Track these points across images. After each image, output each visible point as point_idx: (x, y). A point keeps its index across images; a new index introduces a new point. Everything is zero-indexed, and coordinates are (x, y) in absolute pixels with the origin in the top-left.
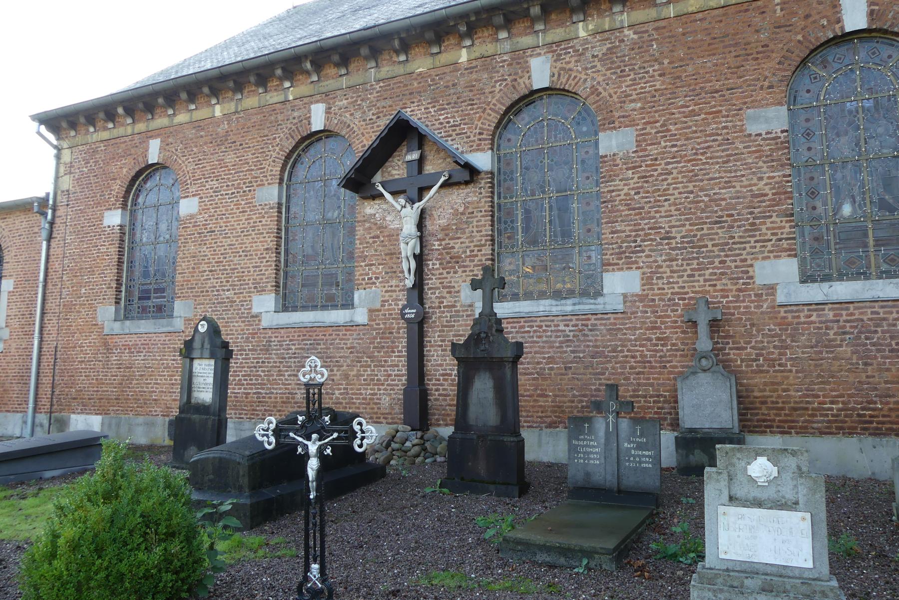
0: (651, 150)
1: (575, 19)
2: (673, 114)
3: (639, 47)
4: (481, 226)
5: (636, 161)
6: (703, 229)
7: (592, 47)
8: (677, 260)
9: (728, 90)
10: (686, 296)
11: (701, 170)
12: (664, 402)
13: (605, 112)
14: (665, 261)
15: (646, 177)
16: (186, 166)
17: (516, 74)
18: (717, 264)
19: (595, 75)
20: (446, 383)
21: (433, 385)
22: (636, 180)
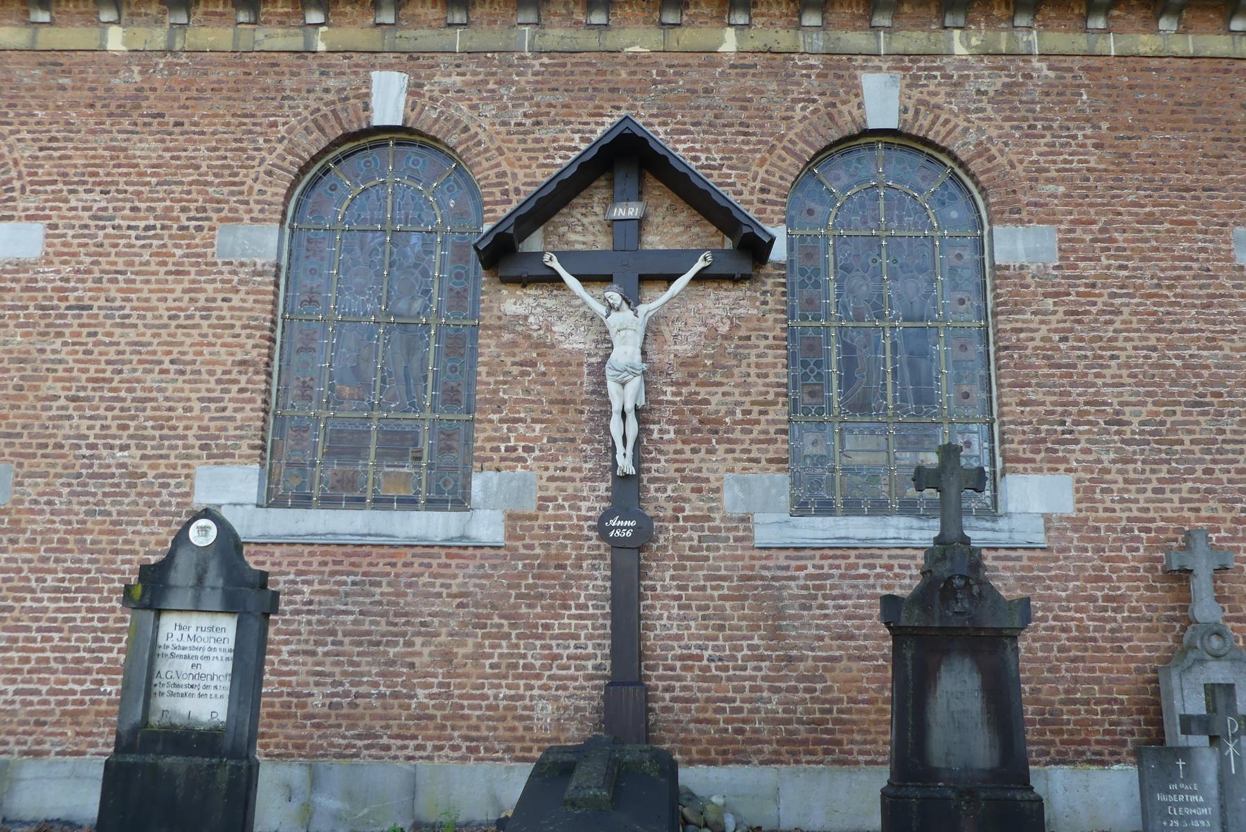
0: (1084, 269)
1: (949, 21)
2: (1120, 214)
3: (1060, 92)
4: (767, 365)
5: (1059, 284)
6: (1174, 413)
7: (977, 77)
8: (1135, 462)
9: (1204, 190)
10: (1153, 526)
11: (1168, 313)
12: (1121, 712)
13: (1003, 190)
14: (1114, 462)
15: (1077, 313)
17: (835, 94)
18: (1199, 474)
19: (984, 125)
20: (689, 675)
21: (660, 678)
22: (1060, 316)
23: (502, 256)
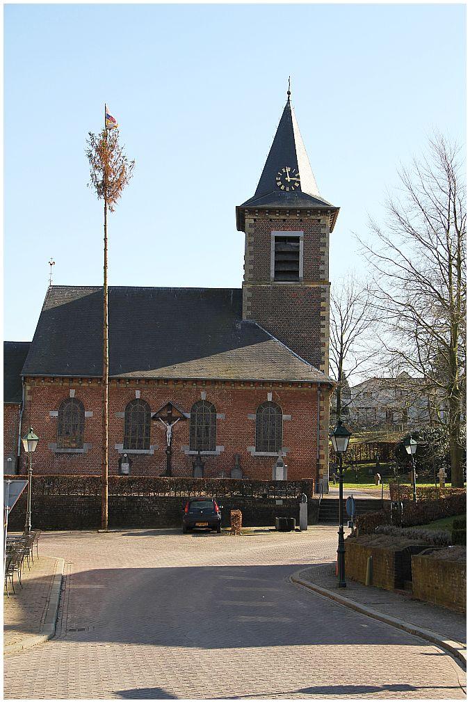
3: (227, 395)
16: (87, 401)
23: (155, 418)
